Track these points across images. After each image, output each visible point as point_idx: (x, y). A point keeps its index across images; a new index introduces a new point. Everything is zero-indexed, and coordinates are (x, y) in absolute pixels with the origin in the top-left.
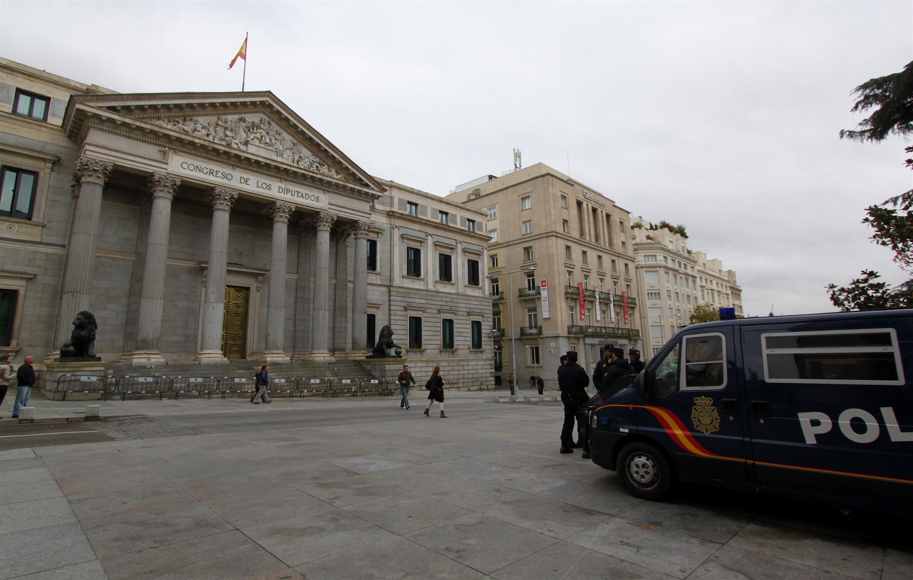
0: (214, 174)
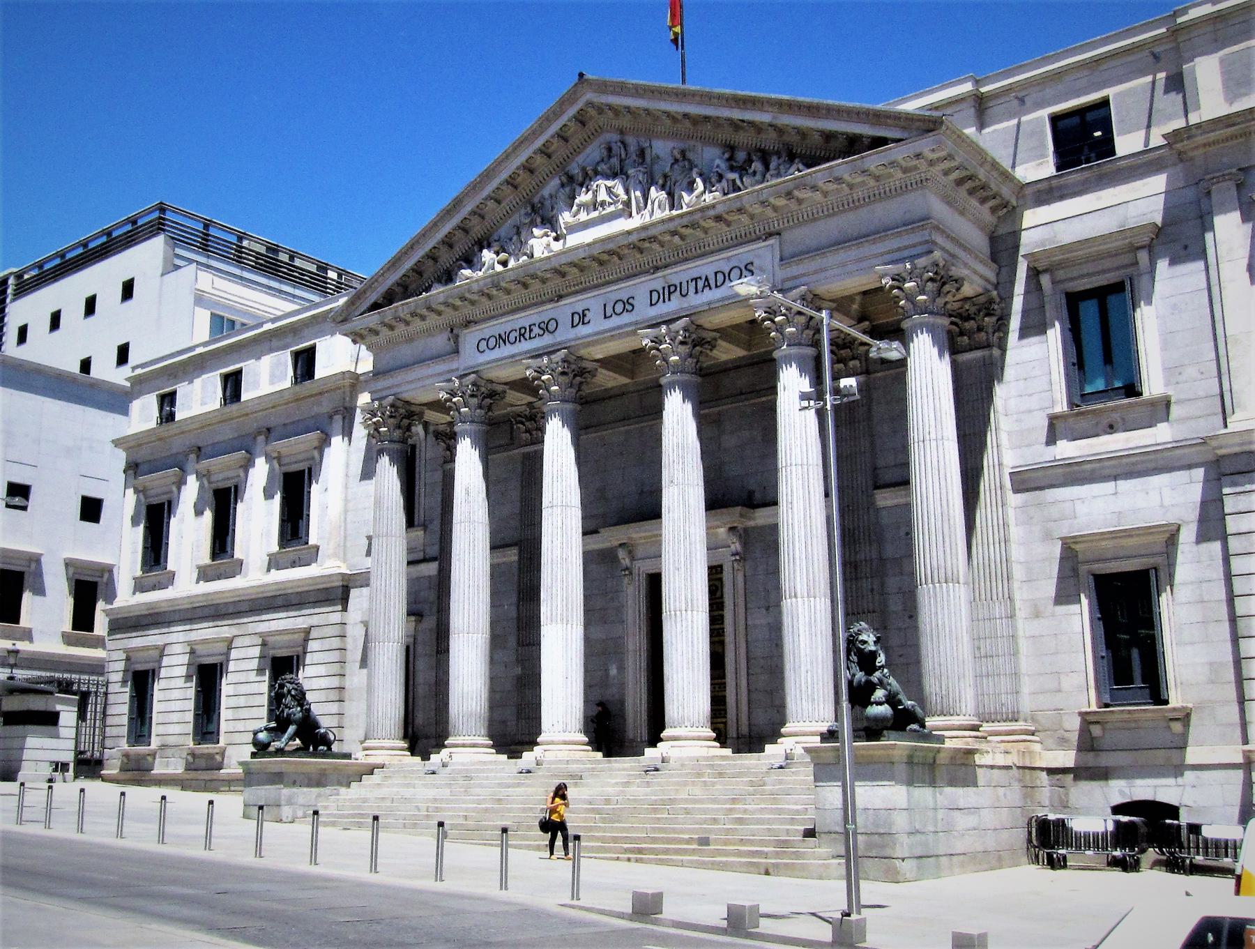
0: (527, 336)
